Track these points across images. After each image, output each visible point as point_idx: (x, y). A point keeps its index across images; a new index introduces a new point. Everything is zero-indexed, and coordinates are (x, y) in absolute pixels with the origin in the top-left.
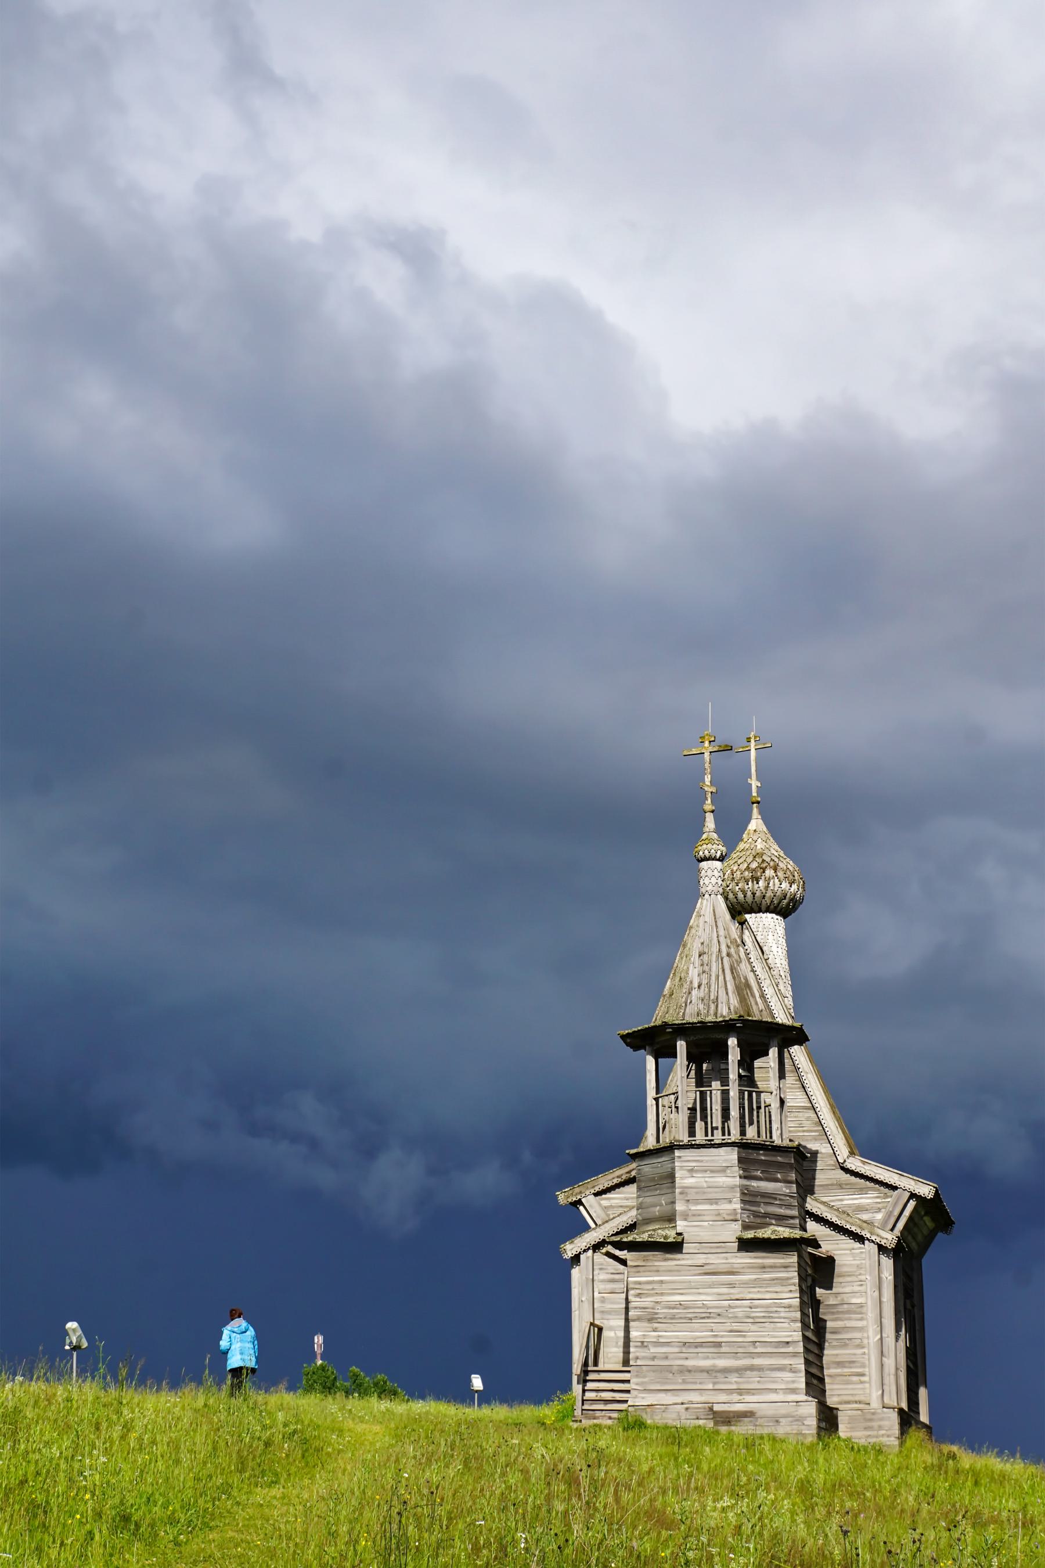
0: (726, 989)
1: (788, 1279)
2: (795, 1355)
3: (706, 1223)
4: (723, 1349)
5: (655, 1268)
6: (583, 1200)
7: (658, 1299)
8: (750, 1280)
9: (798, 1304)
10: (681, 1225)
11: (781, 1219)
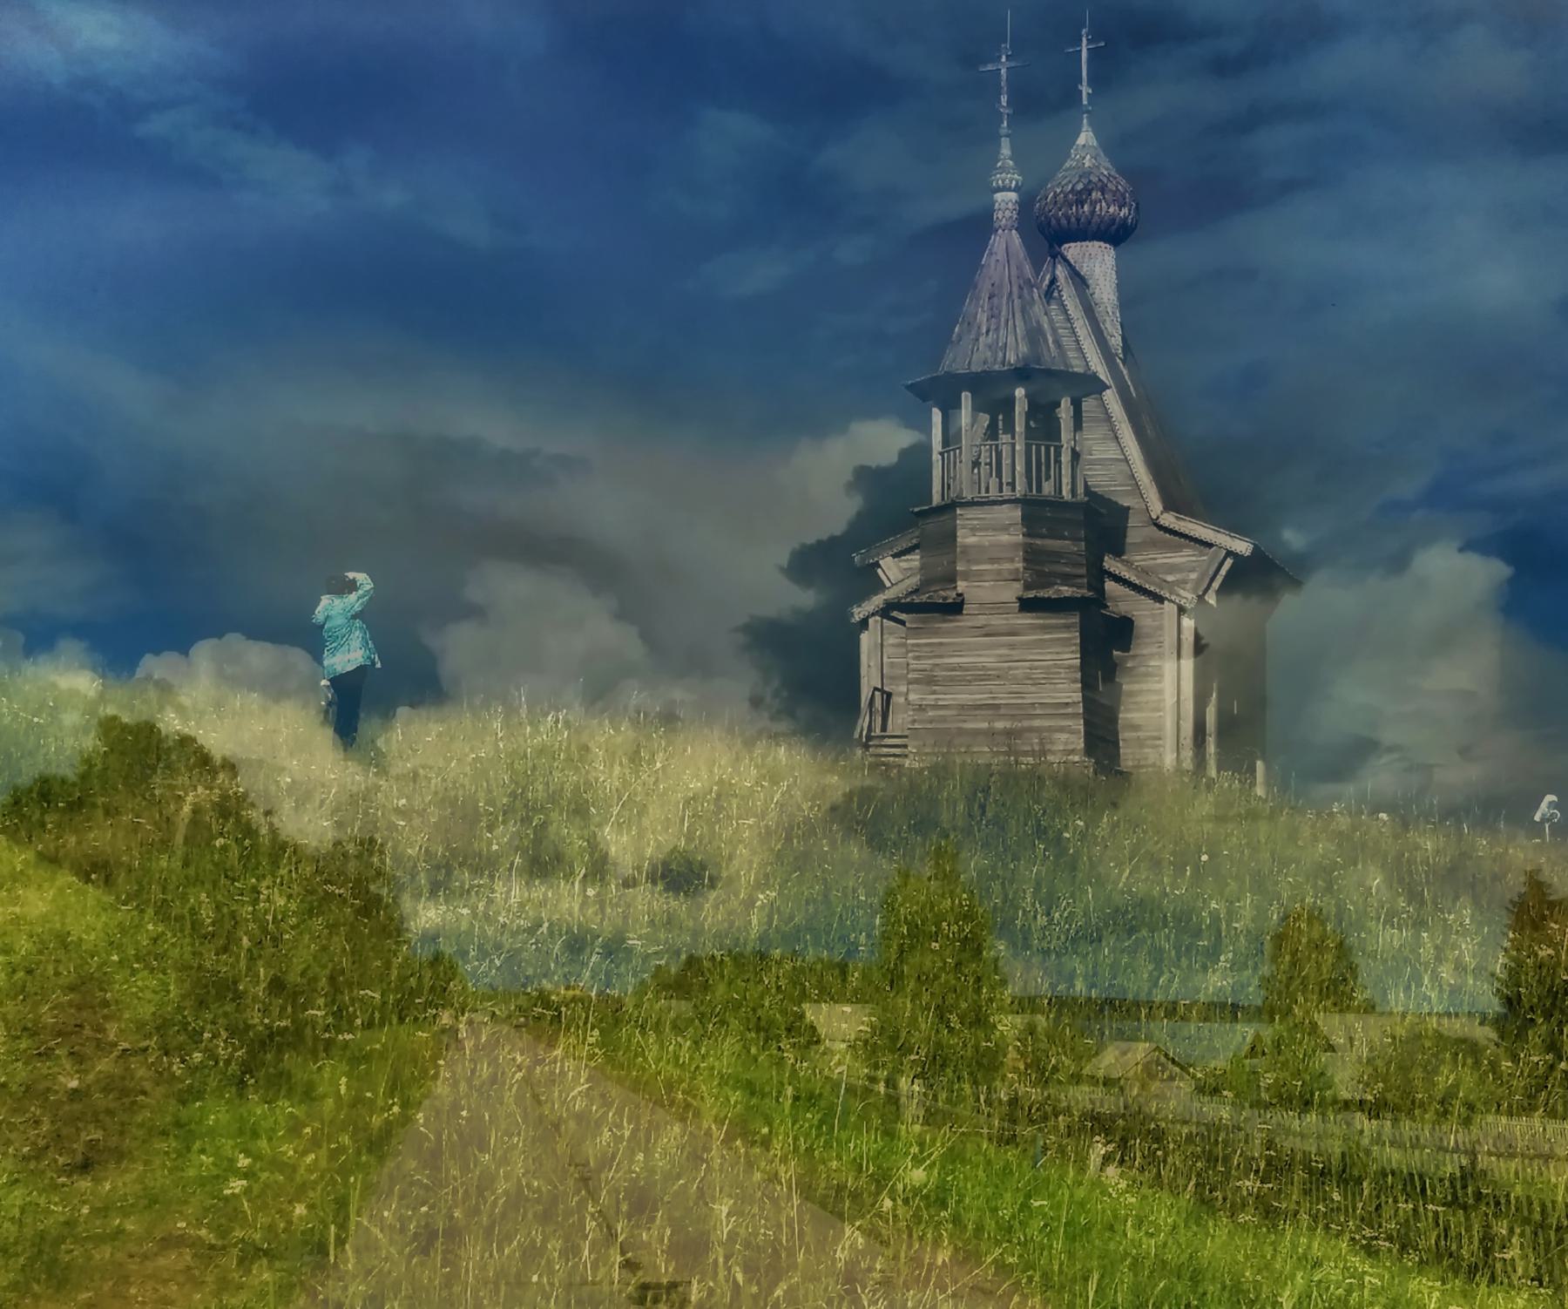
2: (1074, 716)
4: (1002, 711)
10: (961, 585)
11: (1067, 579)
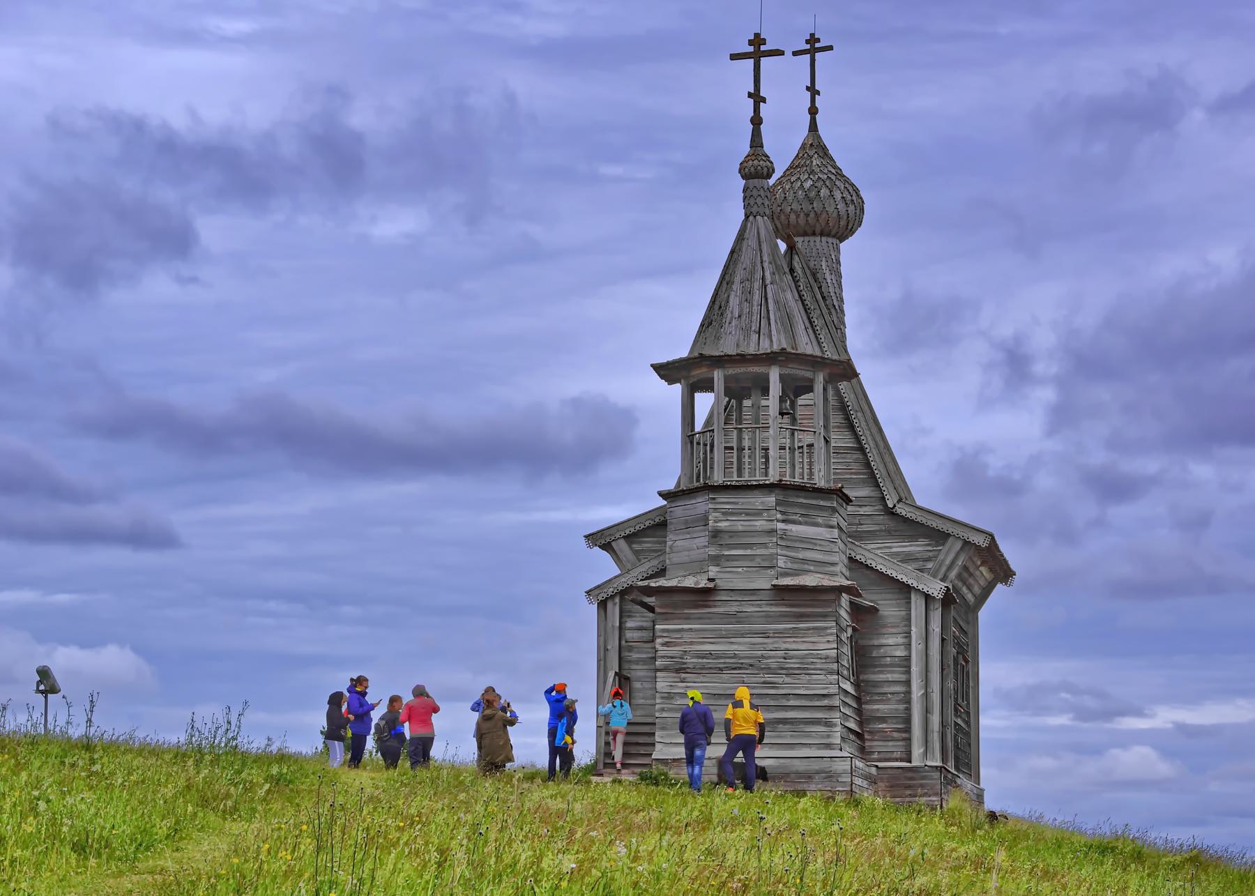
0: (769, 319)
1: (826, 628)
7: (688, 648)
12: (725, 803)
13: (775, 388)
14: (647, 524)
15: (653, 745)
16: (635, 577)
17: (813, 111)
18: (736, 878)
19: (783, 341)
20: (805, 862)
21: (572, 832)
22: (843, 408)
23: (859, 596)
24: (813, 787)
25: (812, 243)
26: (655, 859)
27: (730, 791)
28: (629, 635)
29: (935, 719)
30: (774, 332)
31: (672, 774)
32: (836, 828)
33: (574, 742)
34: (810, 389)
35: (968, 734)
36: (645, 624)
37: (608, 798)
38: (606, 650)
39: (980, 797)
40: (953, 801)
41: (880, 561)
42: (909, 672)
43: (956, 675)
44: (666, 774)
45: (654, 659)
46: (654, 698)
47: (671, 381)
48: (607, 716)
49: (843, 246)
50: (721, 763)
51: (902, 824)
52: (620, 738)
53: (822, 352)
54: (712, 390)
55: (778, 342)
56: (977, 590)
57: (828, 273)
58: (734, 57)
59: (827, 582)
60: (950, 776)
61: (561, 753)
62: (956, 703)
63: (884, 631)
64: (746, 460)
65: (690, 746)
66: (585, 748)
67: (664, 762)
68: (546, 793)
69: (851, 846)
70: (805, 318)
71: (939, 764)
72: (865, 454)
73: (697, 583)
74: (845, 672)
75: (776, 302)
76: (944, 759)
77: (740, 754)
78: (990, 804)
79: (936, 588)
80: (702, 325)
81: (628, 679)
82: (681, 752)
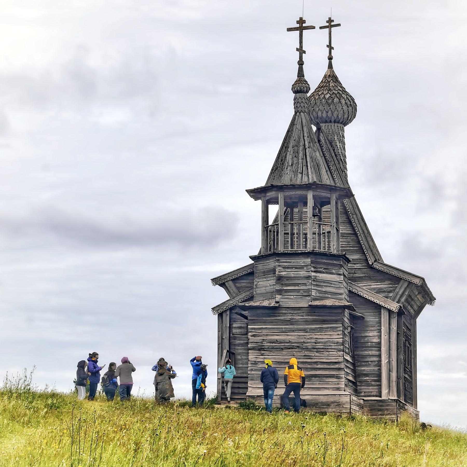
0: (307, 166)
1: (337, 327)
3: (292, 297)
5: (263, 321)
6: (226, 283)
8: (316, 328)
9: (342, 342)
12: (284, 419)
13: (311, 202)
14: (244, 273)
15: (247, 388)
16: (237, 301)
17: (330, 58)
18: (290, 457)
19: (315, 178)
20: (326, 450)
21: (205, 434)
22: (346, 212)
23: (355, 310)
24: (330, 410)
25: (330, 127)
26: (248, 448)
27: (287, 412)
28: (234, 331)
29: (394, 375)
30: (310, 173)
31: (257, 403)
32: (342, 431)
33: (205, 387)
34: (329, 203)
35: (411, 383)
36: (242, 325)
37: (224, 416)
38: (222, 339)
39: (417, 416)
40: (403, 418)
41: (366, 292)
42: (380, 350)
43: (405, 352)
44: (253, 404)
45: (247, 343)
46: (248, 364)
47: (256, 199)
48: (223, 373)
49: (346, 128)
50: (282, 398)
51: (377, 429)
52: (229, 385)
53: (335, 183)
54: (278, 203)
55: (312, 178)
56: (416, 307)
57: (338, 142)
58: (289, 30)
59: (337, 304)
60: (401, 405)
61: (199, 392)
62: (405, 367)
63: (367, 329)
64: (296, 240)
65: (266, 389)
66: (211, 389)
67: (253, 397)
68: (191, 413)
69: (350, 441)
70: (326, 166)
71: (396, 398)
72: (357, 237)
73: (270, 304)
74: (347, 350)
75: (311, 158)
76: (399, 396)
77: (292, 393)
78: (423, 419)
79: (394, 307)
80: (272, 170)
81: (233, 354)
82: (261, 392)
